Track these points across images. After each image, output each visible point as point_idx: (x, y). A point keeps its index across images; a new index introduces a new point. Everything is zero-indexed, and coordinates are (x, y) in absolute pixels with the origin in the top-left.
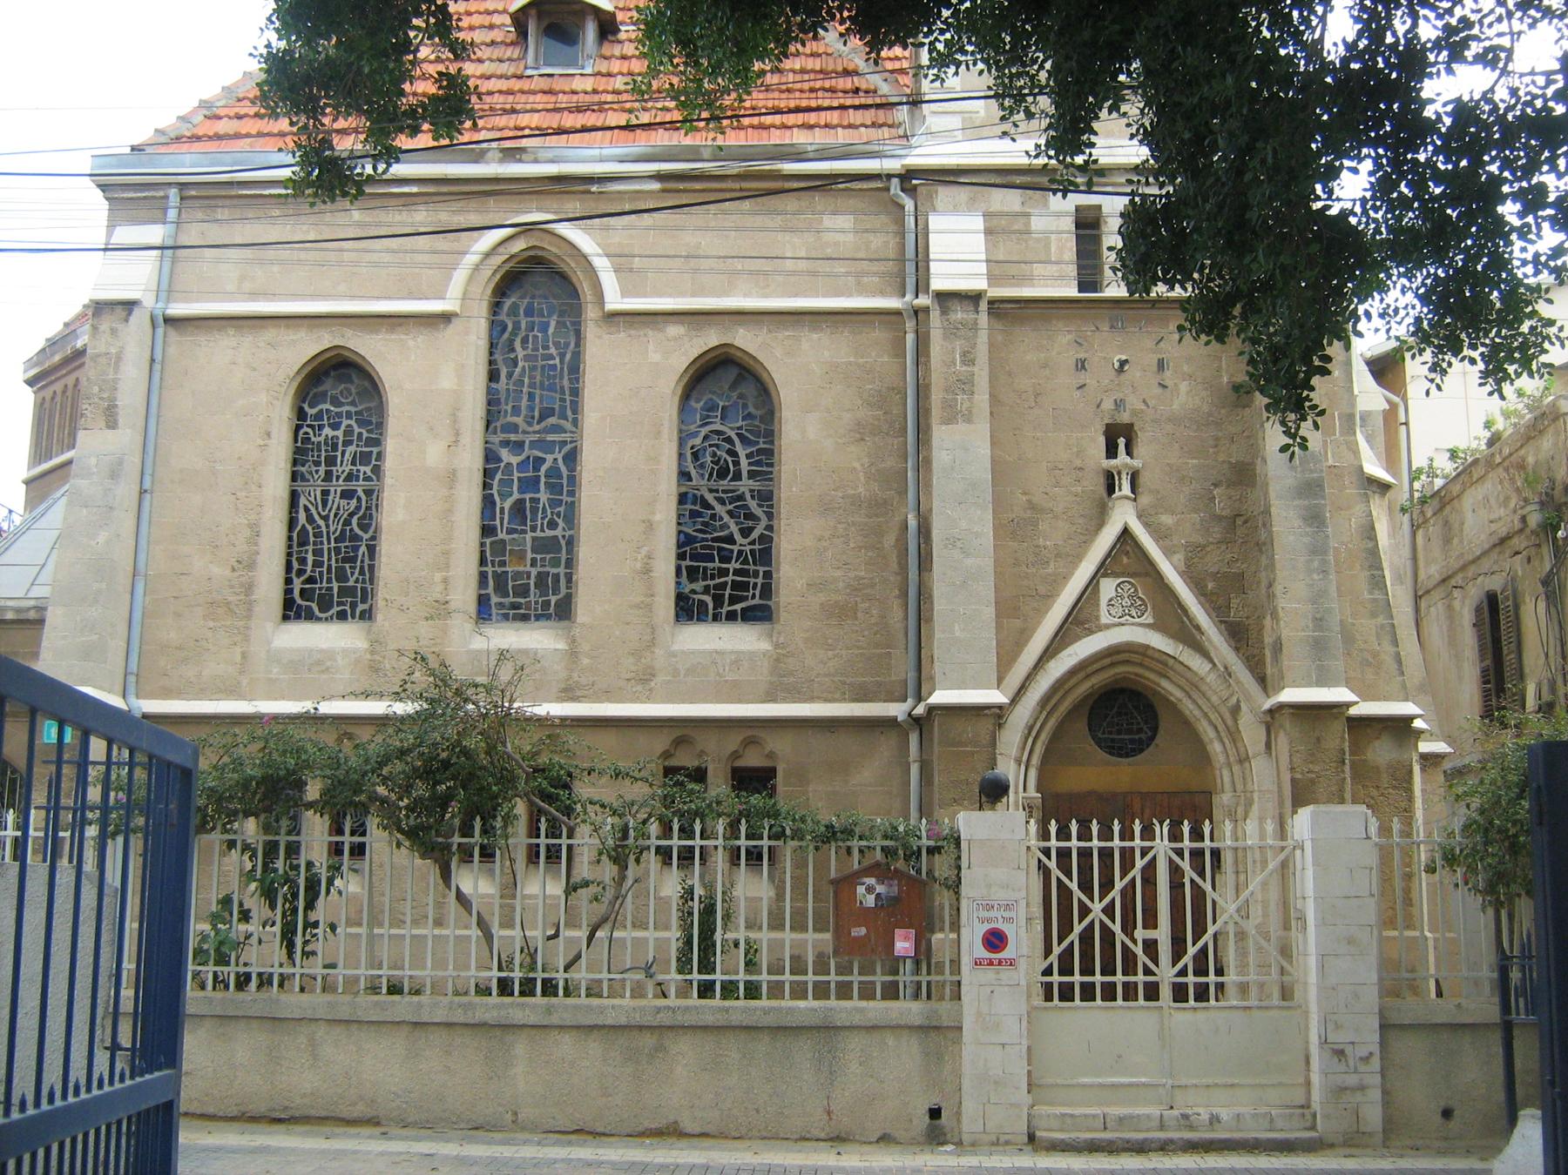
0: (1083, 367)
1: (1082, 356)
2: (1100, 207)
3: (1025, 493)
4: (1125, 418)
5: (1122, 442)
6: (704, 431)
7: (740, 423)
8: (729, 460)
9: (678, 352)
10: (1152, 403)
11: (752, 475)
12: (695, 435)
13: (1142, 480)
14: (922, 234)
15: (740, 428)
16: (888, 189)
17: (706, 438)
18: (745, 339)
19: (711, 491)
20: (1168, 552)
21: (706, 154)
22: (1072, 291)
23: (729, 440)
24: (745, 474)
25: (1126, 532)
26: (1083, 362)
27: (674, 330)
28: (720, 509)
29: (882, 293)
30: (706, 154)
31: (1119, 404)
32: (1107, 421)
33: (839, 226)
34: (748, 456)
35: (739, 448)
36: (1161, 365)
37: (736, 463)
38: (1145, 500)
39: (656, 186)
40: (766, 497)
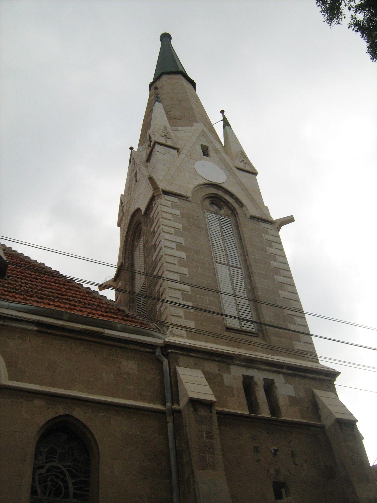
5: (283, 490)
6: (48, 466)
7: (69, 464)
8: (62, 484)
9: (40, 416)
11: (76, 496)
12: (42, 467)
14: (174, 375)
15: (70, 466)
16: (154, 353)
17: (48, 471)
18: (79, 413)
21: (66, 317)
22: (247, 413)
23: (62, 473)
24: (71, 495)
27: (38, 403)
29: (154, 402)
30: (66, 317)
31: (277, 472)
33: (130, 366)
34: (74, 484)
35: (68, 478)
37: (67, 488)
39: (35, 328)
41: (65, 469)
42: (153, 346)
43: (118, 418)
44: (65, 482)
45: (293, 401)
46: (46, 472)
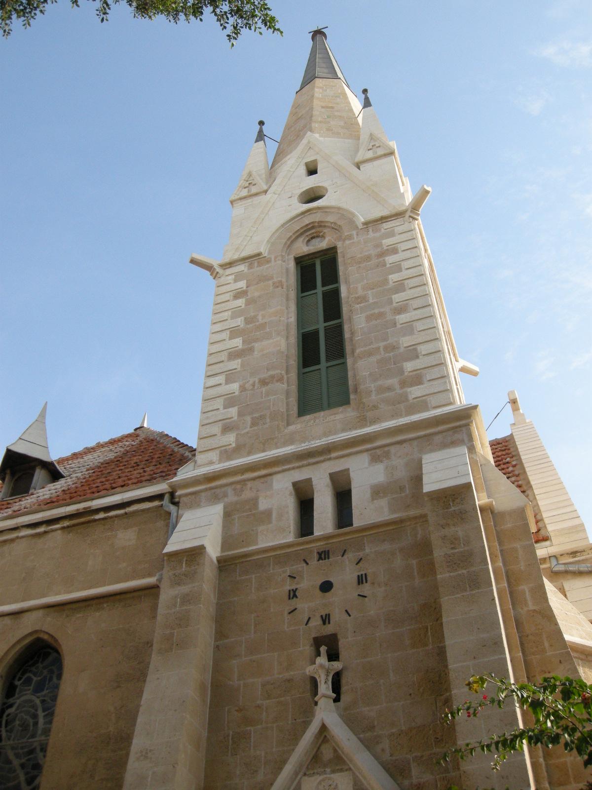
0: (295, 596)
1: (294, 587)
2: (309, 481)
3: (240, 710)
4: (329, 629)
10: (354, 613)
13: (344, 681)
19: (13, 748)
20: (369, 745)
23: (34, 706)
25: (323, 728)
26: (294, 591)
28: (16, 762)
32: (314, 636)
36: (361, 580)
37: (36, 724)
38: (345, 698)
40: (44, 749)
41: (38, 702)
42: (160, 497)
43: (97, 614)
44: (35, 716)
45: (377, 492)
46: (16, 710)
